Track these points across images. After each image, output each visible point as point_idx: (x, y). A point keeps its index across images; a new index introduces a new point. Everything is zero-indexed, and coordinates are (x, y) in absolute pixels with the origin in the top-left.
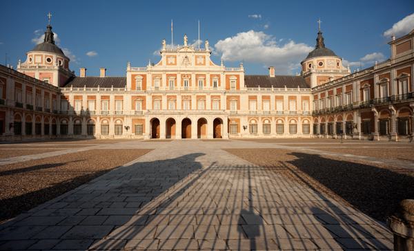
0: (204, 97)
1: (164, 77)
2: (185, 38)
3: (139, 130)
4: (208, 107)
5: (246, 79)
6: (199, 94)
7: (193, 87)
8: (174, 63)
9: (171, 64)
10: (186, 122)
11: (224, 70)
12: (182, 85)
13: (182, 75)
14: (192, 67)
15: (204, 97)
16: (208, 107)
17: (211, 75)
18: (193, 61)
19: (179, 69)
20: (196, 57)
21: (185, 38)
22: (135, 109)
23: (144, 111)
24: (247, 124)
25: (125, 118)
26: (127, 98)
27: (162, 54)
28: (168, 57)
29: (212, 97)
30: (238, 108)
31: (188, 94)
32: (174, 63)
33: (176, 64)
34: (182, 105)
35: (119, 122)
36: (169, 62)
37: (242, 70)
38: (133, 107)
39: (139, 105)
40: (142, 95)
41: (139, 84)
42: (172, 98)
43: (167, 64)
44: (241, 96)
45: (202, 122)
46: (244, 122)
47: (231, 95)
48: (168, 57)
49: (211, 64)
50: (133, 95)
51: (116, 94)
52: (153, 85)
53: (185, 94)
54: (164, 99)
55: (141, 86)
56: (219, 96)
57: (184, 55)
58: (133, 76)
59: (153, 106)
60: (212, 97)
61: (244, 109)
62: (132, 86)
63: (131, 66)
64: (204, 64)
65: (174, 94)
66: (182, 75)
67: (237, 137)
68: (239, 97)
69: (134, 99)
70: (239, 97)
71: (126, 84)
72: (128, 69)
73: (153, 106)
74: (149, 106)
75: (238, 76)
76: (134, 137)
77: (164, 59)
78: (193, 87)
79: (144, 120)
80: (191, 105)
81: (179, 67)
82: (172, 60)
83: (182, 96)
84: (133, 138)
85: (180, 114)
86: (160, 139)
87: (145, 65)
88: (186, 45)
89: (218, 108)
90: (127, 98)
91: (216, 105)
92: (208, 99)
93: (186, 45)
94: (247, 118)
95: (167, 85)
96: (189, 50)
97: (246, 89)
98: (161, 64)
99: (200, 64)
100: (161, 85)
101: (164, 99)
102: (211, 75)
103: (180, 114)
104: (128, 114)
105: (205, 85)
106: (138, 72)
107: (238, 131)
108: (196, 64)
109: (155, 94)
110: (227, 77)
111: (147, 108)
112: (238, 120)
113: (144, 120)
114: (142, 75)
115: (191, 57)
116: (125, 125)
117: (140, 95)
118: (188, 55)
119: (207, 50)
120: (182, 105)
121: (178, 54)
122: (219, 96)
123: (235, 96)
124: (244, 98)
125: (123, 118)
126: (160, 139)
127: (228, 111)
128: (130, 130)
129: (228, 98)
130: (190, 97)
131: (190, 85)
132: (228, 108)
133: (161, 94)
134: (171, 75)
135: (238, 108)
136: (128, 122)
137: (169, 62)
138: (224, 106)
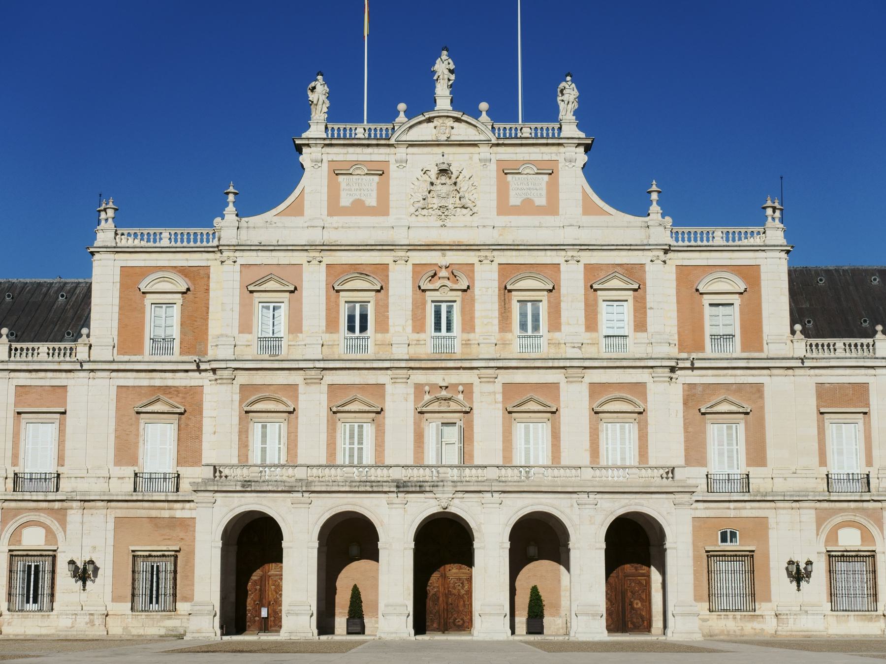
0: (553, 388)
1: (314, 282)
2: (443, 66)
3: (155, 580)
4: (575, 449)
5: (801, 284)
6: (520, 377)
7: (485, 328)
8: (372, 201)
9: (358, 208)
10: (444, 543)
11: (666, 238)
12: (418, 326)
13: (418, 268)
14: (483, 223)
15: (553, 388)
16: (575, 449)
17: (590, 269)
18: (484, 195)
19: (402, 237)
20: (506, 171)
21: (443, 66)
22: (134, 461)
23: (192, 475)
24: (810, 549)
25: (74, 516)
26: (92, 400)
27: (306, 158)
28: (337, 171)
29: (596, 389)
30: (757, 453)
31: (453, 378)
32: (372, 201)
33: (382, 209)
34: (419, 438)
35: (33, 539)
36: (345, 201)
37: (775, 234)
38: (126, 450)
39: (158, 445)
40: (179, 381)
41: (165, 321)
42: (357, 404)
43: (334, 208)
44: (776, 386)
45: (539, 539)
46: (792, 537)
47: (709, 378)
48: (337, 171)
49: (588, 209)
50: (130, 380)
51: (23, 379)
52: (245, 327)
53: (438, 378)
54: (313, 403)
55: (175, 332)
56: (640, 388)
57: (431, 159)
58: (130, 279)
59: (244, 445)
60: (596, 389)
61: (790, 462)
62: (123, 327)
63: (119, 222)
64: (552, 208)
65: (371, 378)
66: (418, 268)
67: (750, 628)
68: (758, 389)
69: (135, 408)
70: (758, 389)
71: (87, 323)
72: (105, 235)
73: (244, 445)
74: (218, 444)
75: (751, 276)
76: (126, 622)
77: (313, 182)
78: (485, 328)
79: (187, 525)
80: (466, 437)
81: (404, 223)
82: (359, 188)
83: (418, 387)
84: (116, 629)
85: (402, 487)
86: (283, 635)
87: (204, 213)
88: (443, 102)
89: (632, 458)
90: (92, 400)
91: (619, 441)
92: (574, 399)
93: (443, 102)
94: (808, 515)
95: (331, 325)
96: (462, 132)
97: (800, 347)
98: (297, 210)
99: (527, 208)
100: (295, 326)
101: (313, 403)
102: (590, 269)
103: (402, 487)
104: (93, 487)
105: (555, 325)
106: (162, 255)
107: (753, 593)
108: (504, 208)
109: (259, 378)
110: (687, 277)
111: (210, 455)
112: (761, 526)
113: (187, 525)
114: (183, 271)
115: (477, 167)
116: (69, 552)
117: (170, 380)
118: (456, 158)
119: (571, 130)
120: (419, 438)
121: (401, 151)
122: (640, 388)
123: (740, 388)
124: (790, 398)
125: (61, 516)
126: (283, 635)
127: (694, 476)
128: (102, 587)
129: (692, 397)
130: (468, 390)
131: (469, 325)
132: (695, 452)
133: (295, 378)
134: (360, 271)
135: (757, 453)
136: (88, 537)
137: (345, 201)
138: (667, 445)
